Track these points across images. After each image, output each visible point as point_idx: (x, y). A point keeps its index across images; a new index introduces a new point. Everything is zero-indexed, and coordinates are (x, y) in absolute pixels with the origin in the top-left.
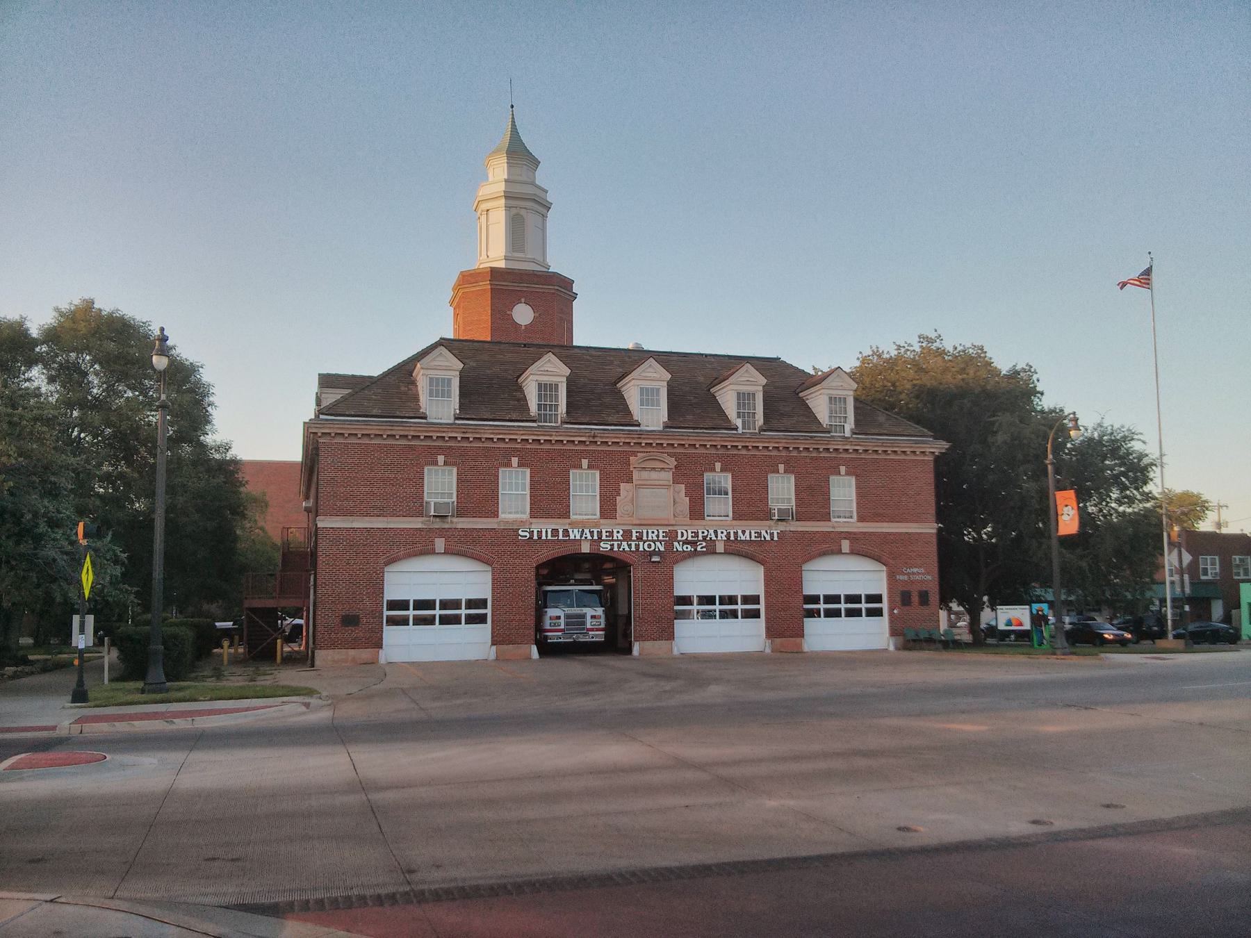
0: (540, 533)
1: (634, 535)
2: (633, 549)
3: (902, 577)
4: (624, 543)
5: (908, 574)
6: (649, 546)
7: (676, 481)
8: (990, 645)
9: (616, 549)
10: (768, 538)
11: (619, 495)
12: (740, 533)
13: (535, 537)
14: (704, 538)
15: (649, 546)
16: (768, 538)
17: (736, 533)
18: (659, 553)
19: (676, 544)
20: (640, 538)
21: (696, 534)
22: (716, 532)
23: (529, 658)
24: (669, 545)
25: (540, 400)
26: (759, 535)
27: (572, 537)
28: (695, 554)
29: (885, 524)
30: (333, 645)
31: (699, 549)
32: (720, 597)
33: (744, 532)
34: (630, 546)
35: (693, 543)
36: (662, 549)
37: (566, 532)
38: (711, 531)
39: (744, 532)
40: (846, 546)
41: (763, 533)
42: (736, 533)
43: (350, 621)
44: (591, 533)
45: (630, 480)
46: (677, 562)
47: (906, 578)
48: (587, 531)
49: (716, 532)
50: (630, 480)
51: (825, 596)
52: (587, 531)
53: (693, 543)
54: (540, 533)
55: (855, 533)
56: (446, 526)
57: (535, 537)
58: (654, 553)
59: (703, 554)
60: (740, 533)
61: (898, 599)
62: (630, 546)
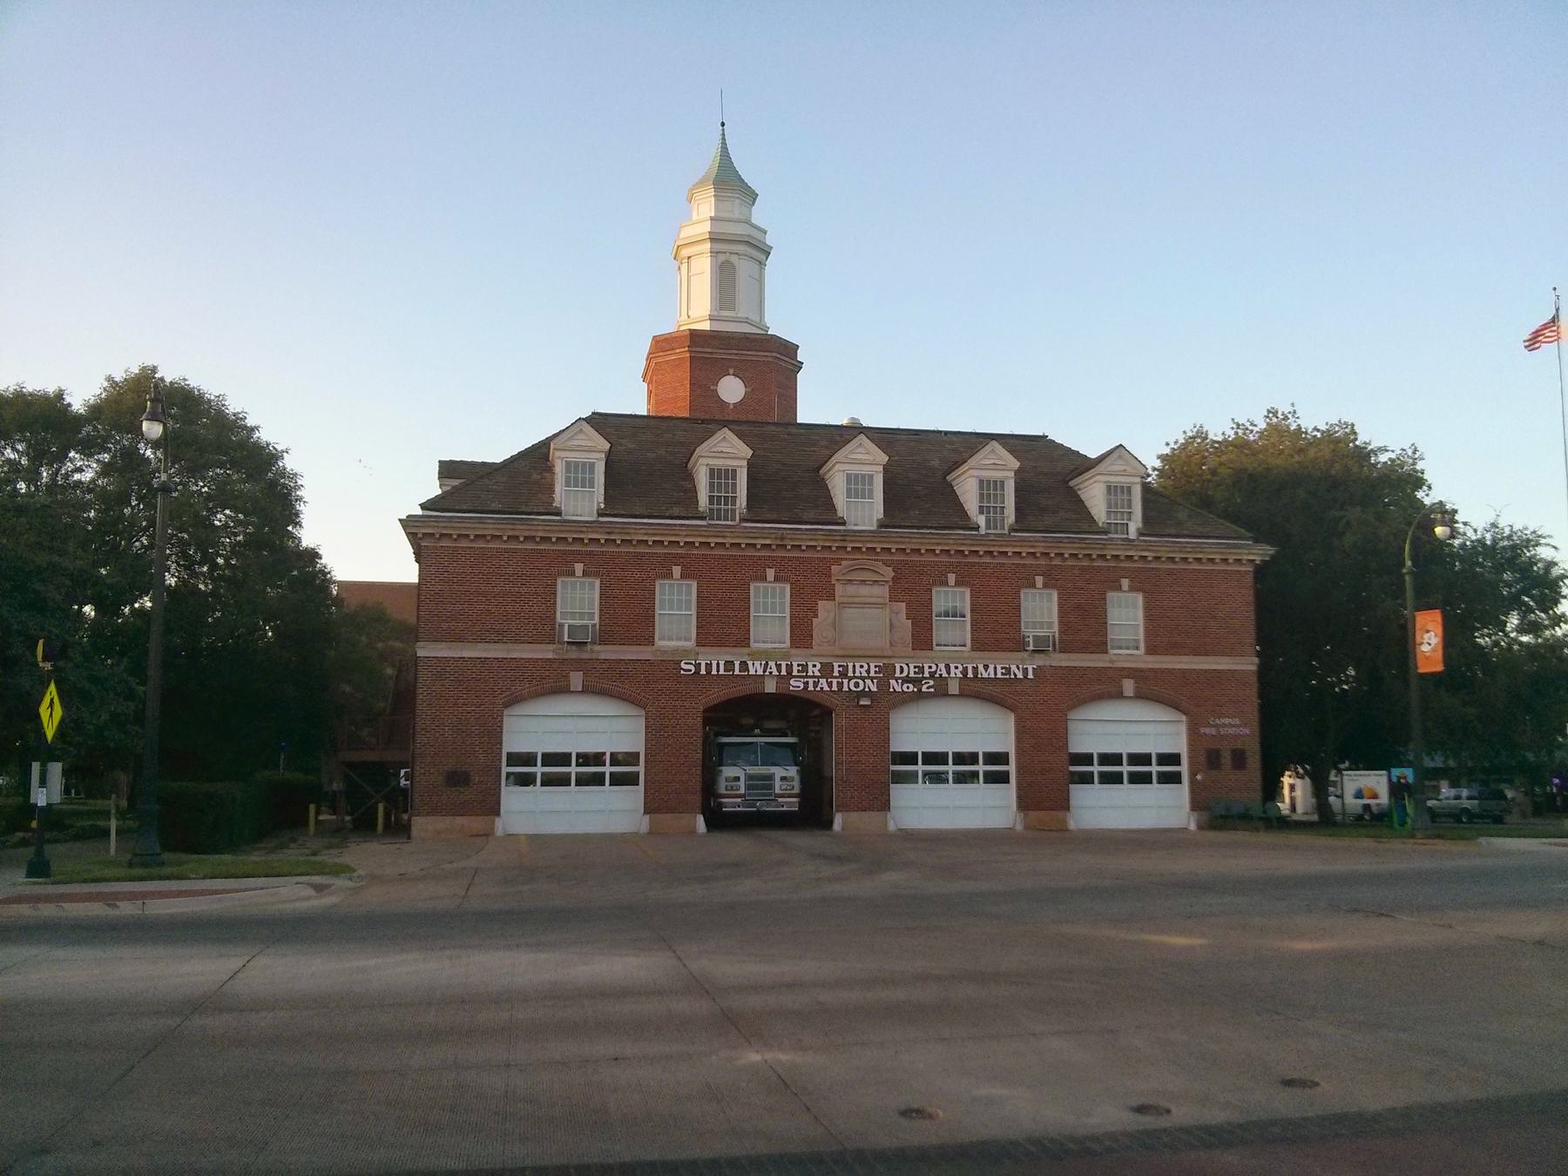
0: (709, 666)
2: (835, 688)
3: (1208, 731)
4: (823, 681)
5: (1216, 726)
6: (857, 685)
9: (811, 688)
10: (1020, 676)
12: (981, 667)
13: (703, 672)
14: (932, 675)
15: (857, 685)
16: (1020, 676)
17: (975, 669)
19: (893, 682)
20: (843, 674)
21: (922, 670)
22: (948, 667)
23: (693, 832)
24: (883, 684)
25: (712, 491)
26: (1008, 670)
27: (752, 672)
28: (919, 696)
29: (1185, 658)
30: (435, 811)
33: (986, 667)
34: (830, 685)
35: (916, 682)
36: (874, 689)
37: (744, 666)
38: (942, 666)
39: (986, 667)
40: (1129, 686)
41: (1014, 668)
42: (975, 669)
43: (457, 779)
44: (779, 667)
45: (831, 596)
46: (894, 706)
47: (1213, 731)
48: (772, 664)
49: (948, 667)
50: (831, 596)
52: (772, 664)
53: (916, 682)
54: (709, 666)
55: (1141, 670)
56: (586, 656)
57: (703, 672)
58: (863, 694)
59: (929, 696)
60: (981, 667)
61: (1203, 759)
62: (830, 685)
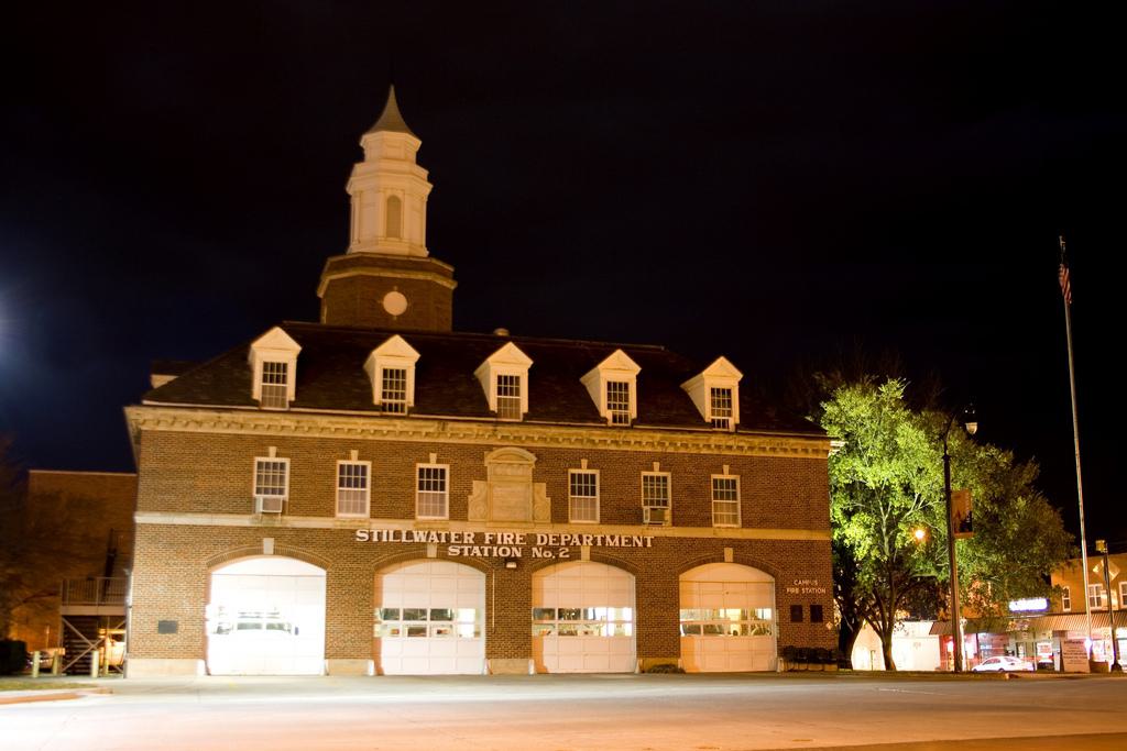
0: (380, 534)
1: (487, 538)
2: (486, 554)
3: (792, 590)
4: (476, 548)
5: (800, 587)
6: (504, 551)
7: (536, 479)
8: (830, 673)
9: (466, 554)
10: (640, 544)
11: (471, 493)
12: (608, 539)
13: (375, 539)
14: (567, 543)
15: (504, 551)
16: (640, 544)
17: (603, 539)
18: (515, 559)
19: (535, 549)
20: (493, 542)
21: (558, 539)
22: (580, 537)
23: (364, 675)
24: (527, 551)
25: (385, 387)
26: (630, 540)
27: (417, 540)
28: (557, 560)
29: (774, 531)
30: (148, 654)
31: (561, 555)
32: (433, 611)
33: (612, 538)
34: (482, 551)
35: (555, 550)
36: (519, 555)
37: (410, 535)
38: (576, 537)
39: (612, 538)
40: (729, 553)
41: (635, 538)
42: (603, 539)
43: (167, 627)
44: (439, 536)
45: (483, 476)
46: (536, 570)
47: (797, 590)
48: (433, 533)
49: (580, 537)
50: (483, 476)
51: (433, 611)
52: (433, 533)
53: (555, 550)
54: (380, 534)
55: (739, 540)
56: (277, 525)
57: (375, 539)
58: (509, 559)
59: (565, 560)
60: (608, 539)
61: (788, 614)
62: (482, 551)
